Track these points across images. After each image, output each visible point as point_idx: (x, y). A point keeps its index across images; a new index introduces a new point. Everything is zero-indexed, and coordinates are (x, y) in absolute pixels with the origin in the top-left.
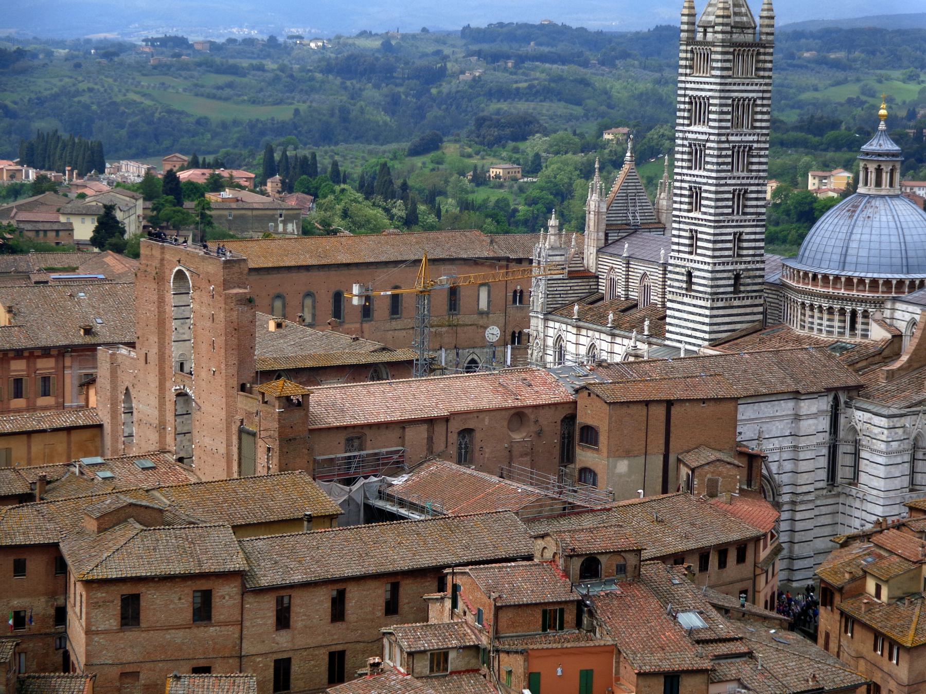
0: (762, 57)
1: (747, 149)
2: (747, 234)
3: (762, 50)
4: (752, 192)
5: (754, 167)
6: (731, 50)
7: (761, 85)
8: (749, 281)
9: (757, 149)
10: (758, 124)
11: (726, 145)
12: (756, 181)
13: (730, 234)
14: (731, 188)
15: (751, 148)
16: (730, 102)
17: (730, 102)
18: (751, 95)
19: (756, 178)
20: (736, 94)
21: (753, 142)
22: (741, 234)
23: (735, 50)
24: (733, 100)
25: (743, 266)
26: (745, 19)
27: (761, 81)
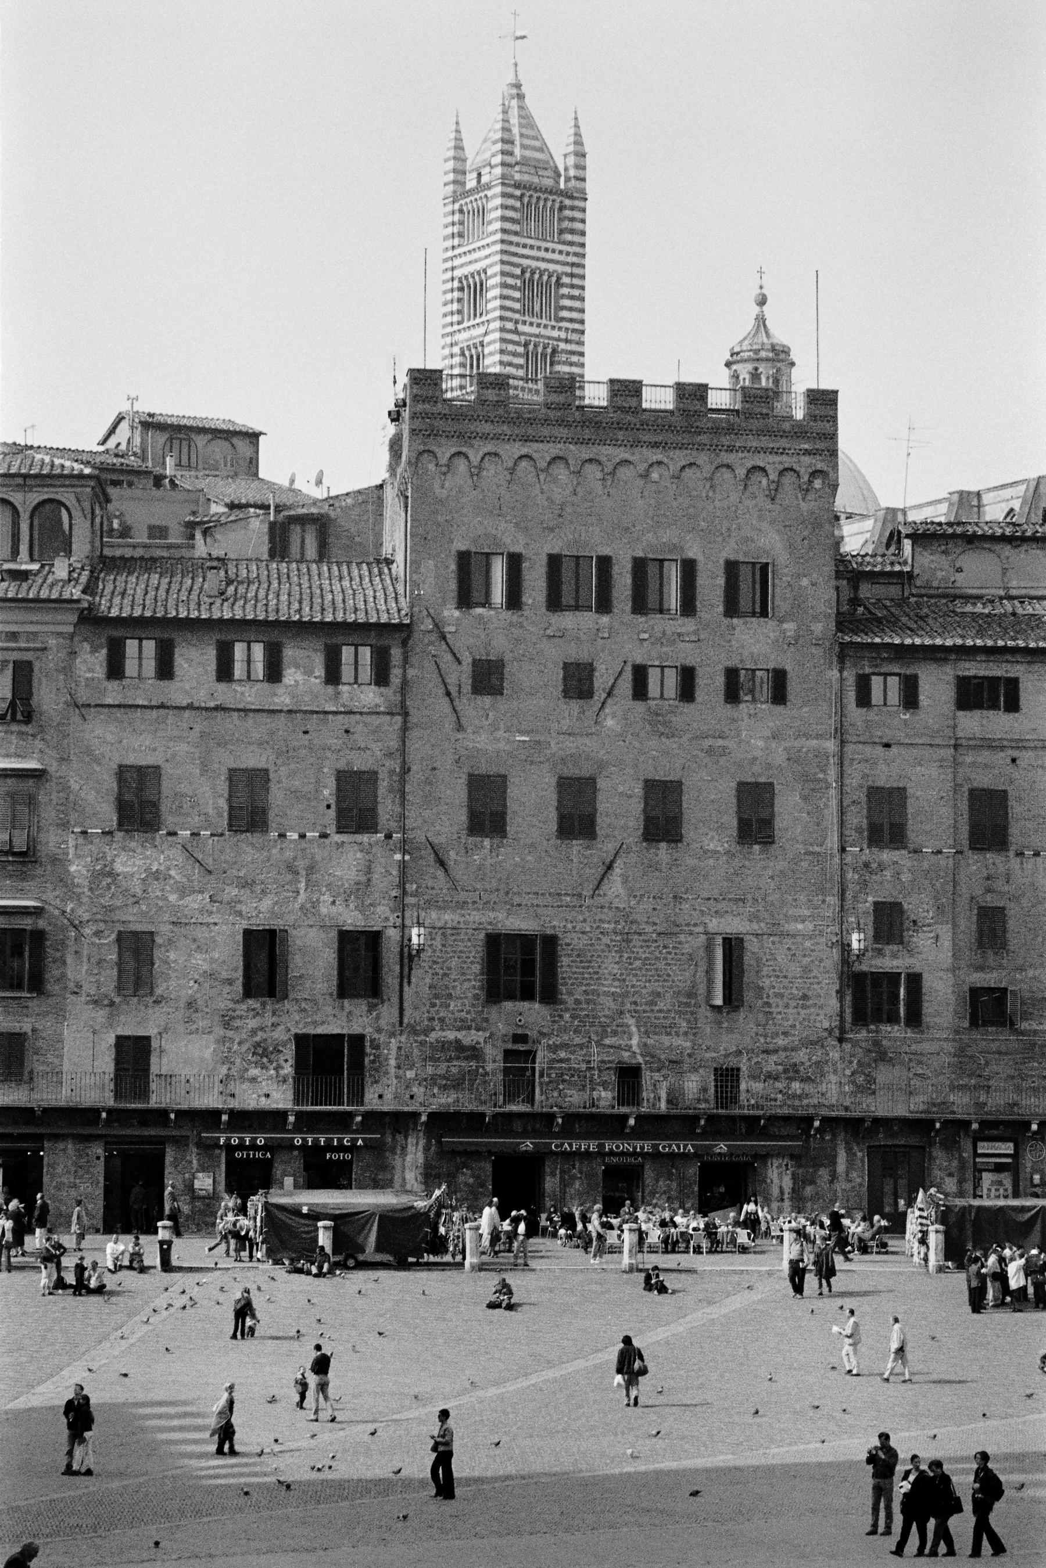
0: (567, 213)
1: (549, 350)
3: (567, 202)
6: (518, 193)
7: (568, 254)
9: (563, 351)
10: (565, 314)
15: (554, 351)
18: (551, 267)
20: (526, 262)
21: (559, 339)
23: (522, 195)
24: (523, 272)
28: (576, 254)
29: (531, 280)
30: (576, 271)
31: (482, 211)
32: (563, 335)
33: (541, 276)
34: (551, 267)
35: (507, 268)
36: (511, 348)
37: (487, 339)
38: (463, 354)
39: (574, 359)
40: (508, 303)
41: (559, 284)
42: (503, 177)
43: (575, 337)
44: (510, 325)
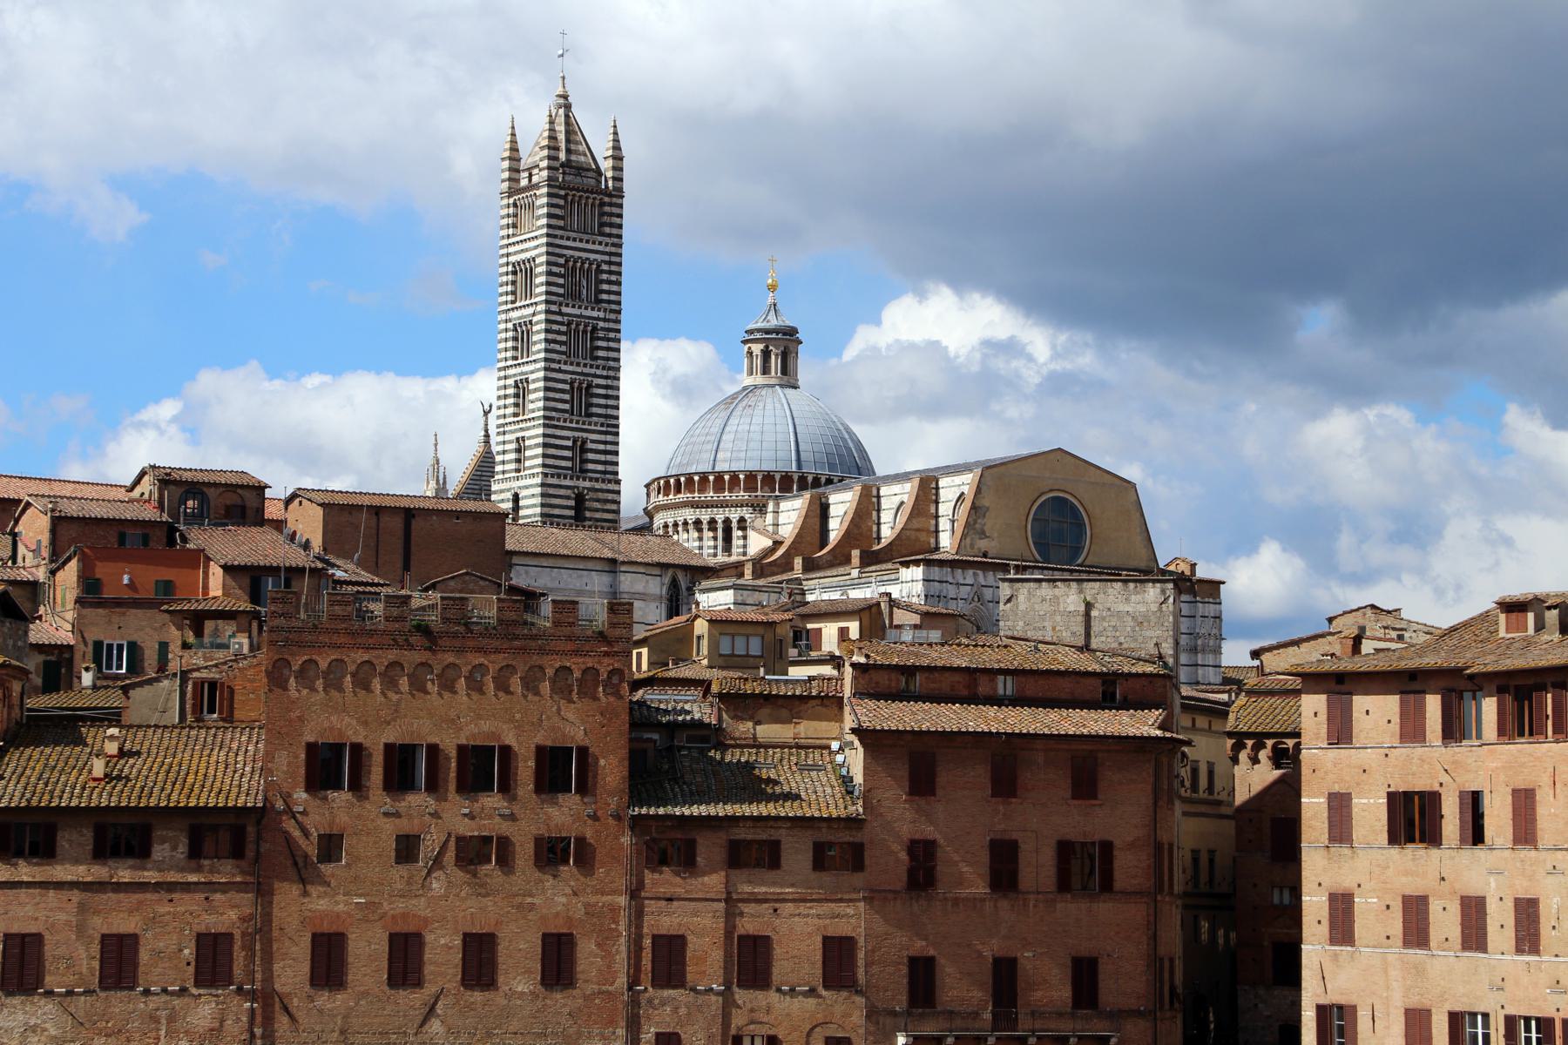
0: (607, 209)
1: (589, 328)
2: (593, 441)
3: (606, 199)
4: (598, 386)
5: (601, 353)
6: (562, 193)
8: (597, 505)
9: (603, 329)
10: (605, 297)
11: (559, 318)
12: (605, 373)
13: (568, 438)
14: (568, 377)
15: (595, 329)
16: (562, 261)
17: (562, 261)
18: (592, 256)
19: (604, 368)
20: (569, 253)
21: (598, 319)
22: (584, 442)
23: (567, 195)
24: (567, 261)
25: (587, 484)
26: (582, 159)
27: (607, 240)
28: (614, 245)
29: (574, 267)
30: (614, 259)
31: (532, 207)
32: (601, 315)
33: (583, 263)
34: (592, 256)
35: (553, 259)
36: (555, 327)
37: (535, 319)
38: (515, 330)
39: (612, 335)
40: (554, 289)
41: (599, 271)
42: (550, 179)
43: (613, 316)
44: (554, 308)
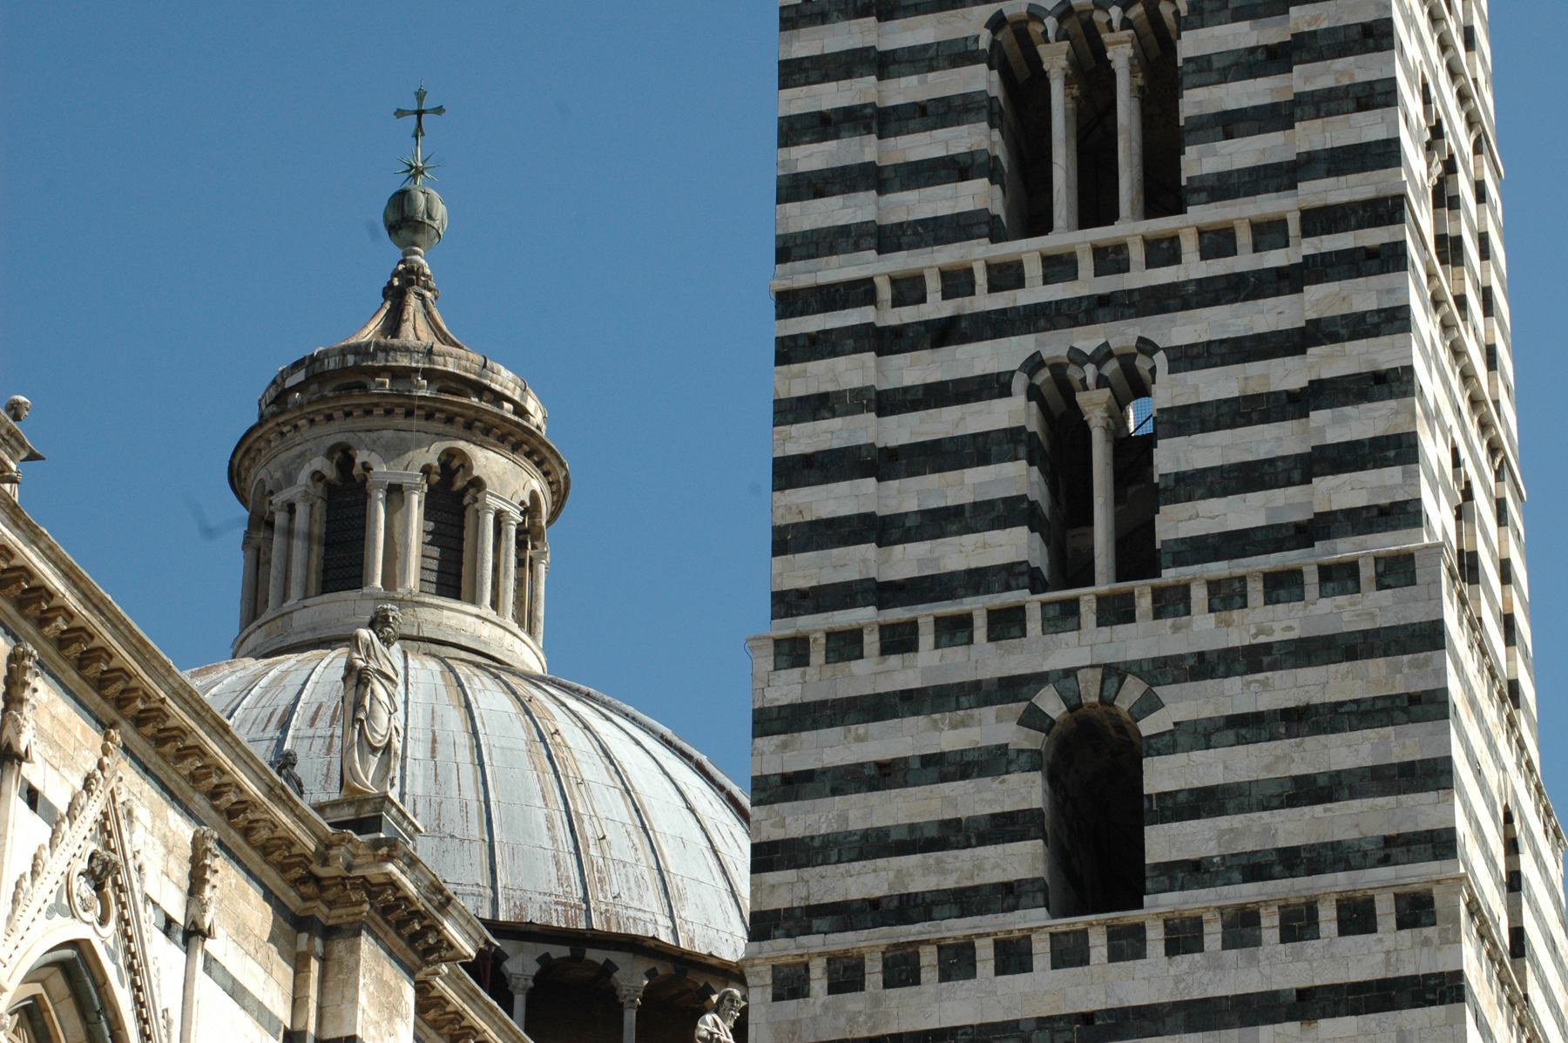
2: (1187, 358)
13: (993, 386)
